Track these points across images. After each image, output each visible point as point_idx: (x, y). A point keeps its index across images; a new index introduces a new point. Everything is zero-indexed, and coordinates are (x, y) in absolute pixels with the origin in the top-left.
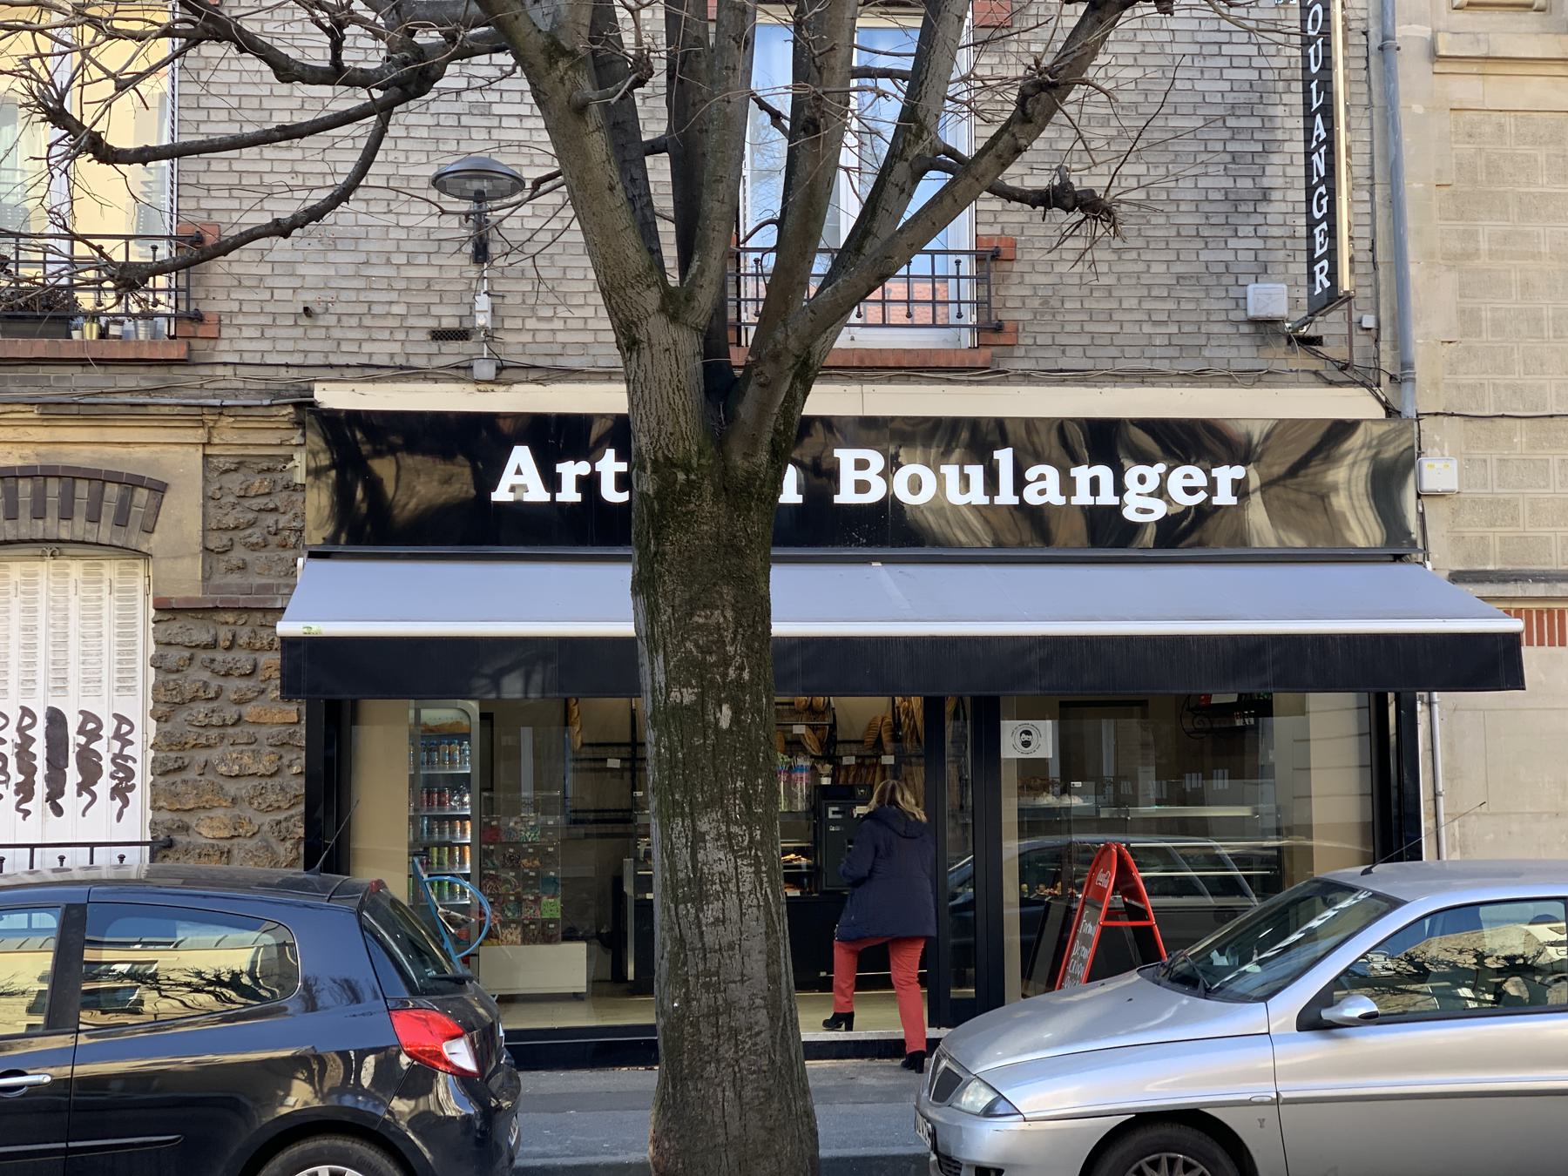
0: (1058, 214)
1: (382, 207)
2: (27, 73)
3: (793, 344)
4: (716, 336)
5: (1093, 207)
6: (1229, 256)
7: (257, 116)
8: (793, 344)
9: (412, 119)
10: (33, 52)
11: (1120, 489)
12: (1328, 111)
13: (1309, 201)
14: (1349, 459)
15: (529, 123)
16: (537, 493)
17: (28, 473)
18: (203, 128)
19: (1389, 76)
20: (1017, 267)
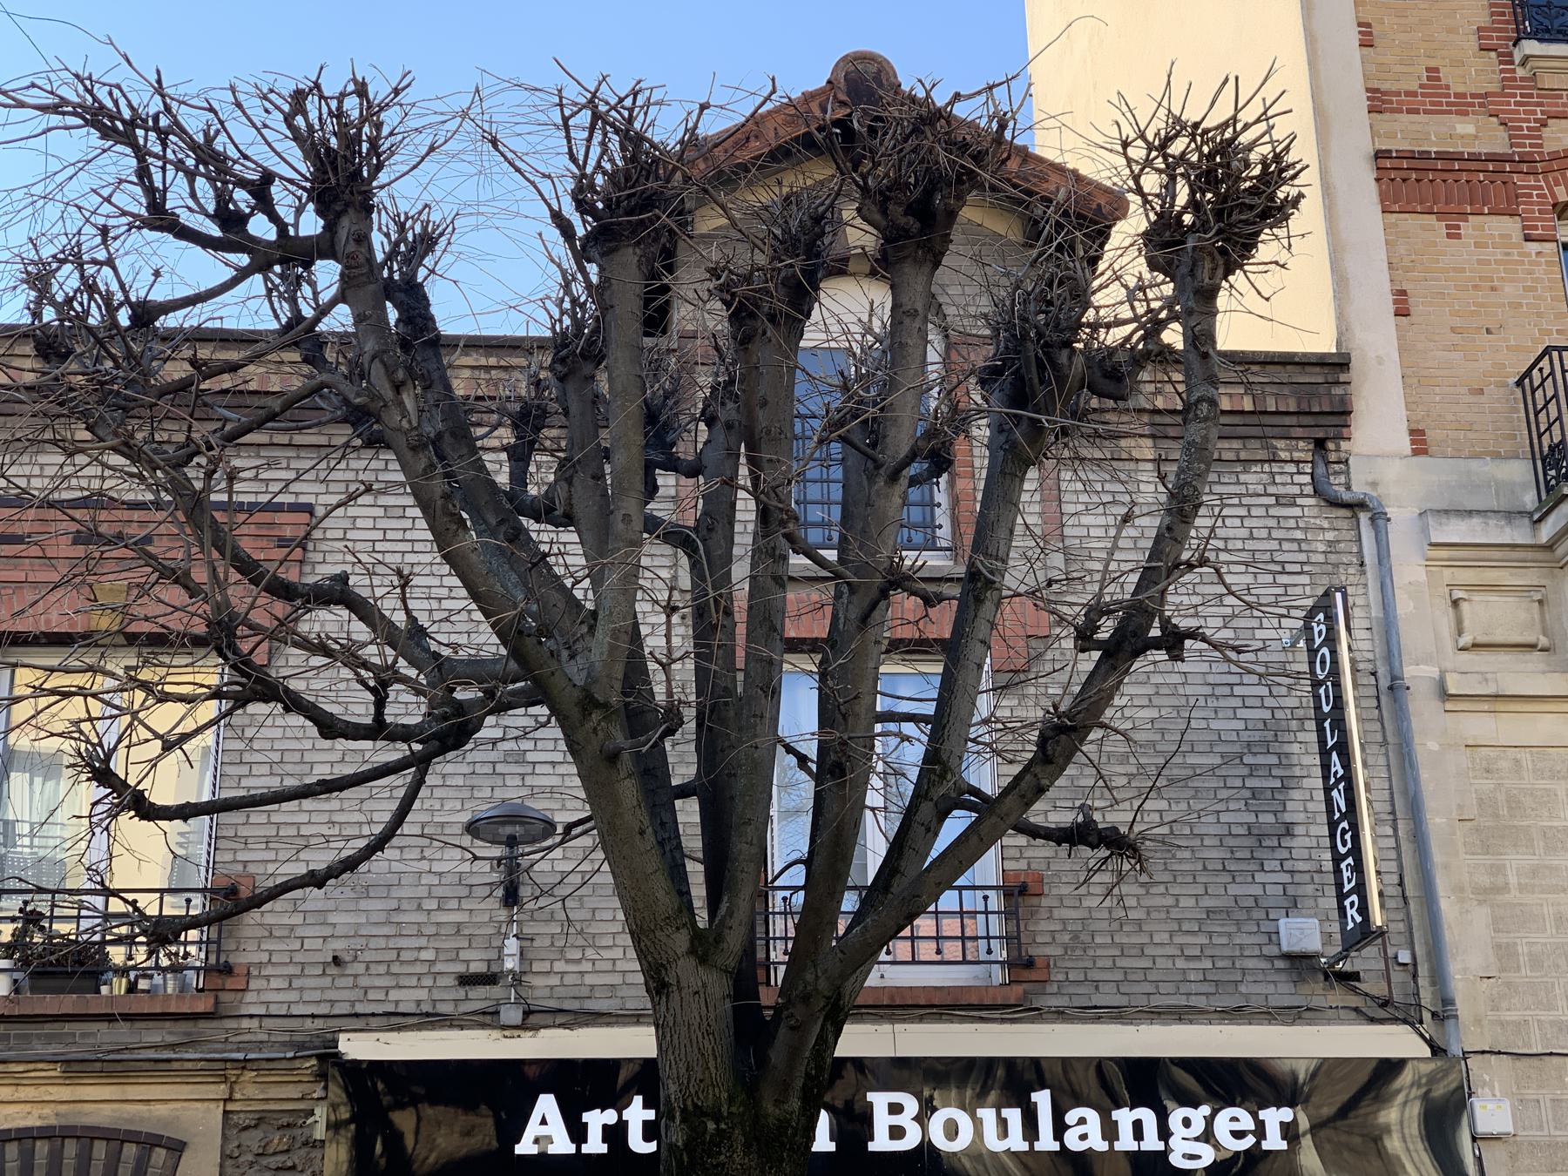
0: (1085, 851)
1: (415, 854)
2: (76, 735)
3: (823, 985)
4: (747, 974)
5: (1118, 843)
6: (1258, 890)
7: (298, 769)
8: (823, 985)
9: (449, 768)
10: (84, 715)
11: (1164, 1133)
12: (1343, 749)
13: (1332, 836)
14: (1400, 1098)
15: (561, 769)
16: (562, 1145)
17: (46, 1133)
18: (244, 783)
19: (1401, 715)
20: (1045, 902)
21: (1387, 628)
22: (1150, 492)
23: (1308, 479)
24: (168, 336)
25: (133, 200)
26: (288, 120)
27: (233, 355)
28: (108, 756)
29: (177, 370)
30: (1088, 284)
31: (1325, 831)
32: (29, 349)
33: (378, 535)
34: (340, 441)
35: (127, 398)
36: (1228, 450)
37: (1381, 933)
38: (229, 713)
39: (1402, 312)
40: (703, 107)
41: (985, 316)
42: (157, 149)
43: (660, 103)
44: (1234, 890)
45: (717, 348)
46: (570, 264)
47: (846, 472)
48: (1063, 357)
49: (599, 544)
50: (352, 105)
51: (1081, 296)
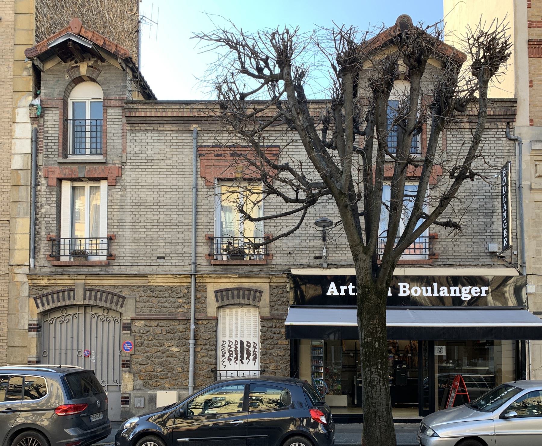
0: (449, 228)
1: (304, 229)
3: (391, 259)
4: (375, 257)
5: (456, 226)
6: (485, 237)
7: (280, 210)
8: (391, 259)
9: (311, 210)
11: (460, 292)
12: (507, 203)
13: (502, 224)
14: (509, 286)
15: (334, 210)
16: (336, 293)
17: (236, 289)
18: (269, 213)
19: (520, 194)
20: (438, 240)
21: (519, 173)
22: (468, 137)
23: (504, 133)
24: (247, 102)
25: (238, 65)
26: (271, 41)
27: (261, 107)
28: (243, 207)
29: (249, 112)
30: (457, 79)
31: (501, 223)
33: (294, 153)
34: (285, 129)
35: (241, 119)
36: (487, 125)
37: (511, 247)
38: (266, 197)
39: (531, 86)
40: (367, 32)
41: (432, 90)
42: (242, 51)
43: (357, 32)
44: (480, 237)
45: (369, 101)
46: (335, 78)
47: (398, 134)
48: (450, 101)
49: (343, 153)
50: (285, 35)
51: (455, 82)
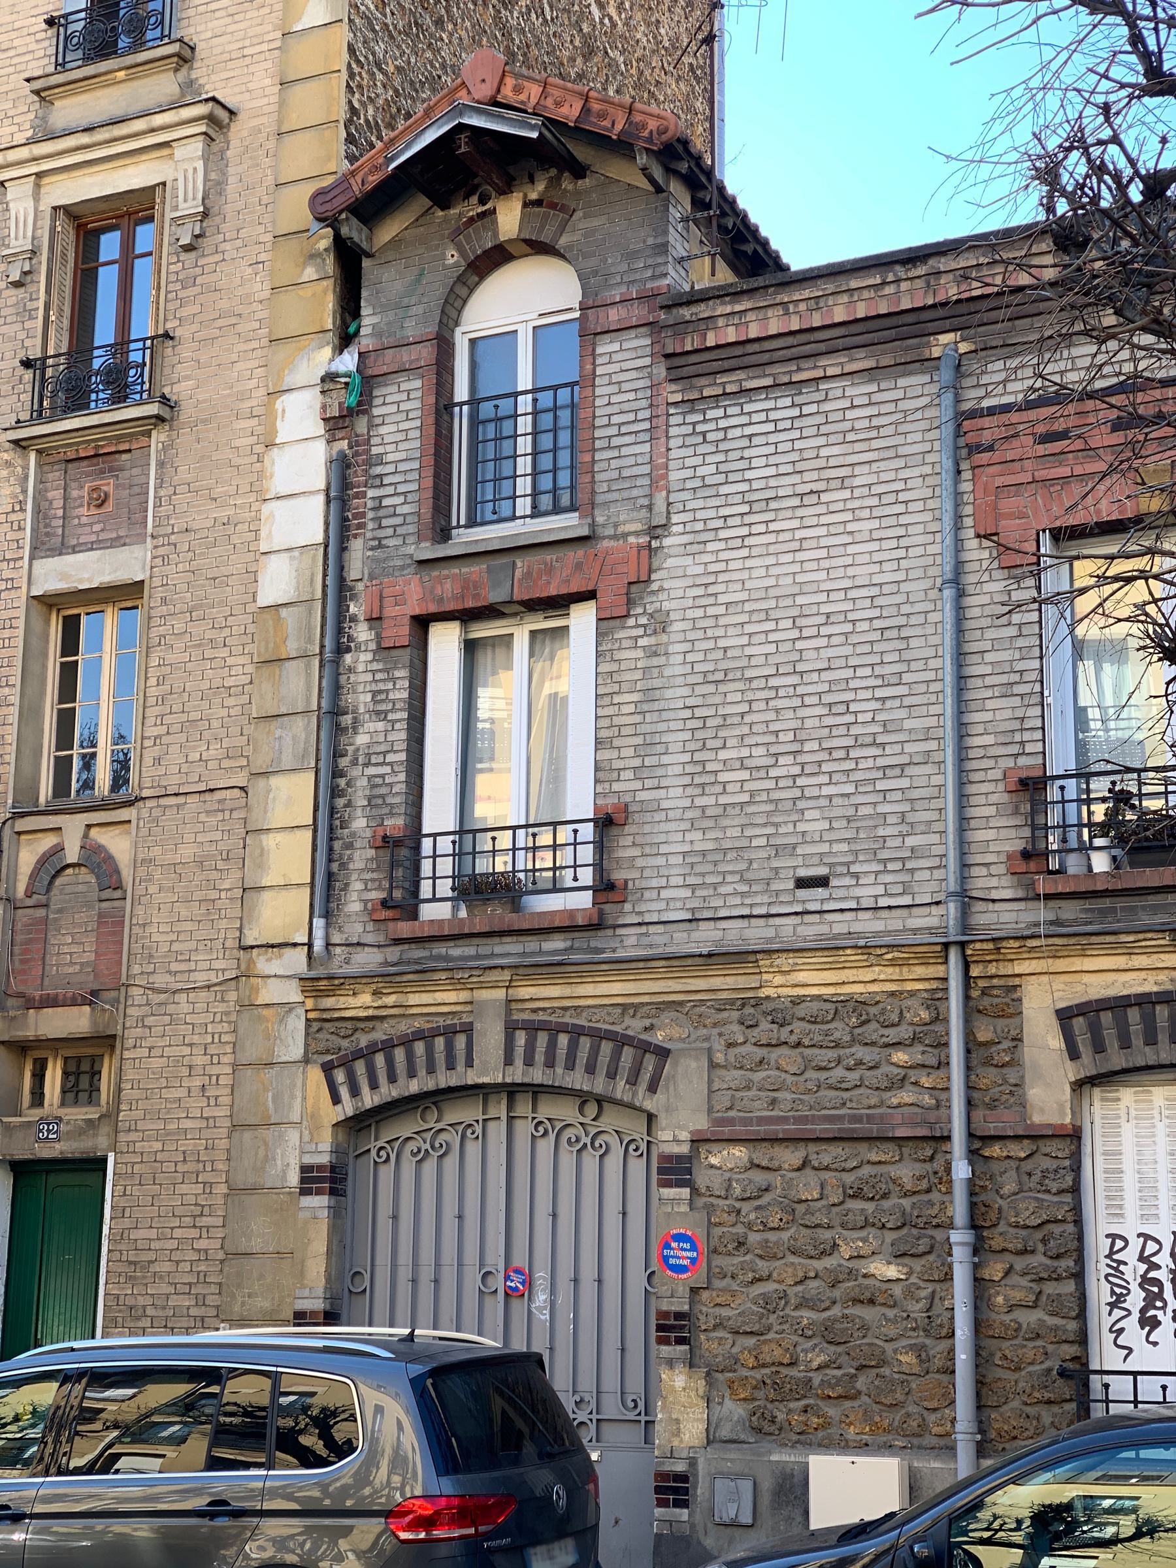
2: (1143, 618)
10: (1148, 598)
25: (1130, 70)
32: (1046, 244)
42: (1148, 11)
